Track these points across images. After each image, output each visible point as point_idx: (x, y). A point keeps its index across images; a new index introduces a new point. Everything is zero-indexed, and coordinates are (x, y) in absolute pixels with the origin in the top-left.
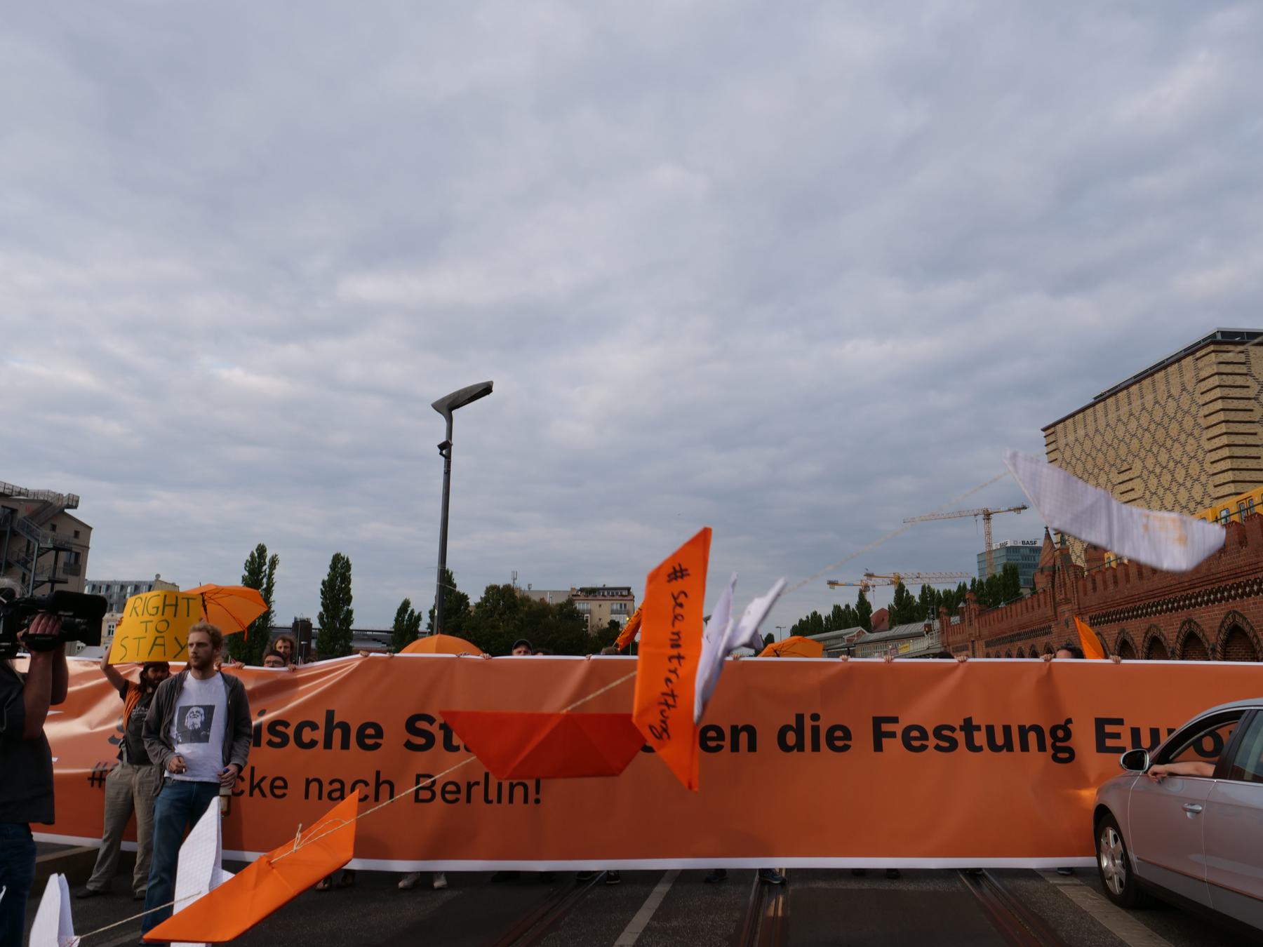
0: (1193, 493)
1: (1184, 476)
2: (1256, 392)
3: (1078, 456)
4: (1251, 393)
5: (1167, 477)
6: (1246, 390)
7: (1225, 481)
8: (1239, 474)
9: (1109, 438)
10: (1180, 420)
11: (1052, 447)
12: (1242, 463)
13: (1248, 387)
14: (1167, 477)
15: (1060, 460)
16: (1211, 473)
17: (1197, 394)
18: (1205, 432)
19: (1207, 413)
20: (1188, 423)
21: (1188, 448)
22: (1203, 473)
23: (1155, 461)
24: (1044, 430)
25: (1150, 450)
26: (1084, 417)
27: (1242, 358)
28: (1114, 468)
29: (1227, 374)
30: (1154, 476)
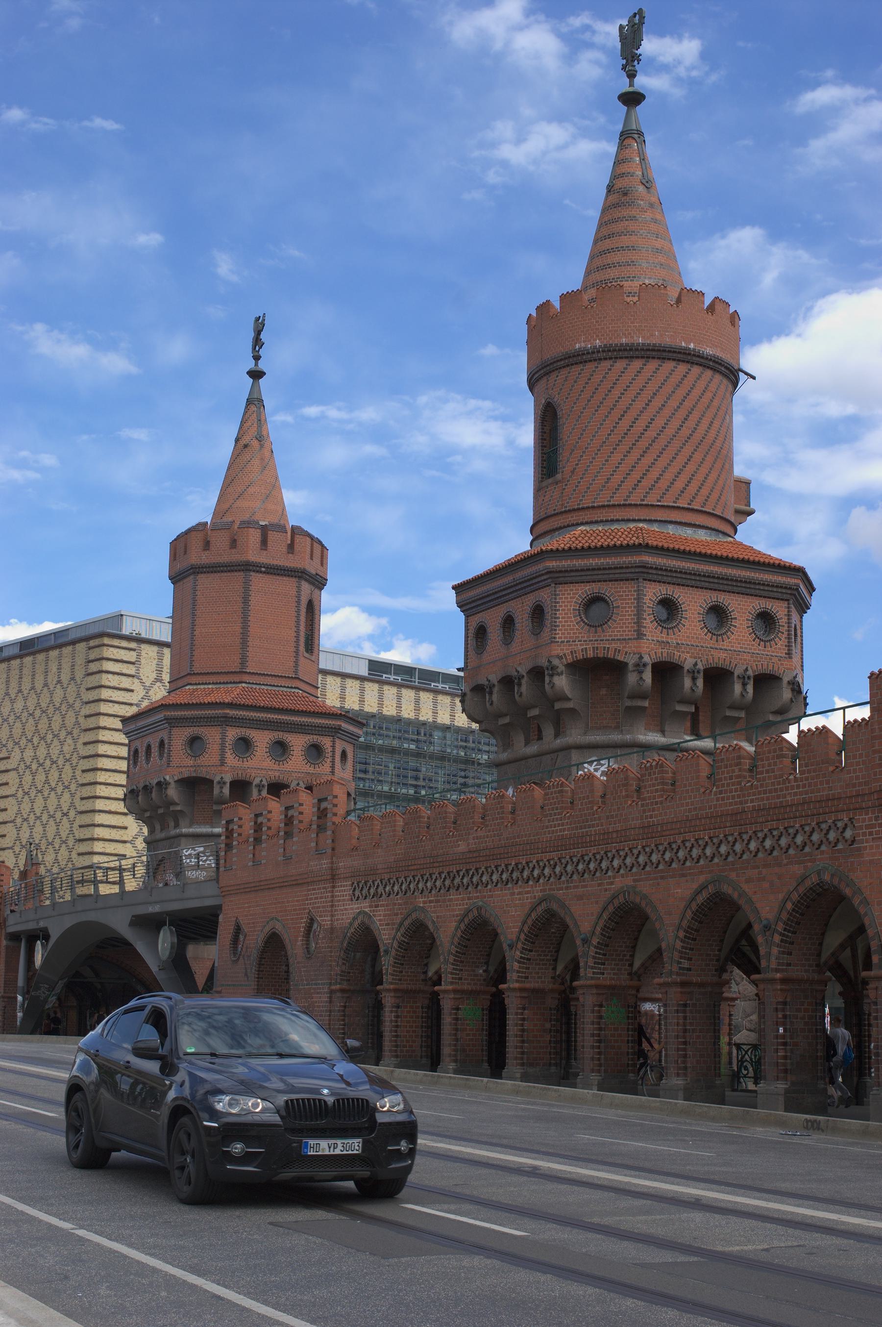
0: (62, 801)
2: (140, 698)
4: (134, 698)
5: (41, 777)
6: (130, 694)
8: (105, 789)
13: (132, 691)
14: (41, 777)
17: (83, 689)
18: (82, 734)
19: (88, 713)
21: (66, 748)
22: (74, 781)
23: (33, 754)
27: (131, 656)
29: (114, 673)
30: (29, 773)
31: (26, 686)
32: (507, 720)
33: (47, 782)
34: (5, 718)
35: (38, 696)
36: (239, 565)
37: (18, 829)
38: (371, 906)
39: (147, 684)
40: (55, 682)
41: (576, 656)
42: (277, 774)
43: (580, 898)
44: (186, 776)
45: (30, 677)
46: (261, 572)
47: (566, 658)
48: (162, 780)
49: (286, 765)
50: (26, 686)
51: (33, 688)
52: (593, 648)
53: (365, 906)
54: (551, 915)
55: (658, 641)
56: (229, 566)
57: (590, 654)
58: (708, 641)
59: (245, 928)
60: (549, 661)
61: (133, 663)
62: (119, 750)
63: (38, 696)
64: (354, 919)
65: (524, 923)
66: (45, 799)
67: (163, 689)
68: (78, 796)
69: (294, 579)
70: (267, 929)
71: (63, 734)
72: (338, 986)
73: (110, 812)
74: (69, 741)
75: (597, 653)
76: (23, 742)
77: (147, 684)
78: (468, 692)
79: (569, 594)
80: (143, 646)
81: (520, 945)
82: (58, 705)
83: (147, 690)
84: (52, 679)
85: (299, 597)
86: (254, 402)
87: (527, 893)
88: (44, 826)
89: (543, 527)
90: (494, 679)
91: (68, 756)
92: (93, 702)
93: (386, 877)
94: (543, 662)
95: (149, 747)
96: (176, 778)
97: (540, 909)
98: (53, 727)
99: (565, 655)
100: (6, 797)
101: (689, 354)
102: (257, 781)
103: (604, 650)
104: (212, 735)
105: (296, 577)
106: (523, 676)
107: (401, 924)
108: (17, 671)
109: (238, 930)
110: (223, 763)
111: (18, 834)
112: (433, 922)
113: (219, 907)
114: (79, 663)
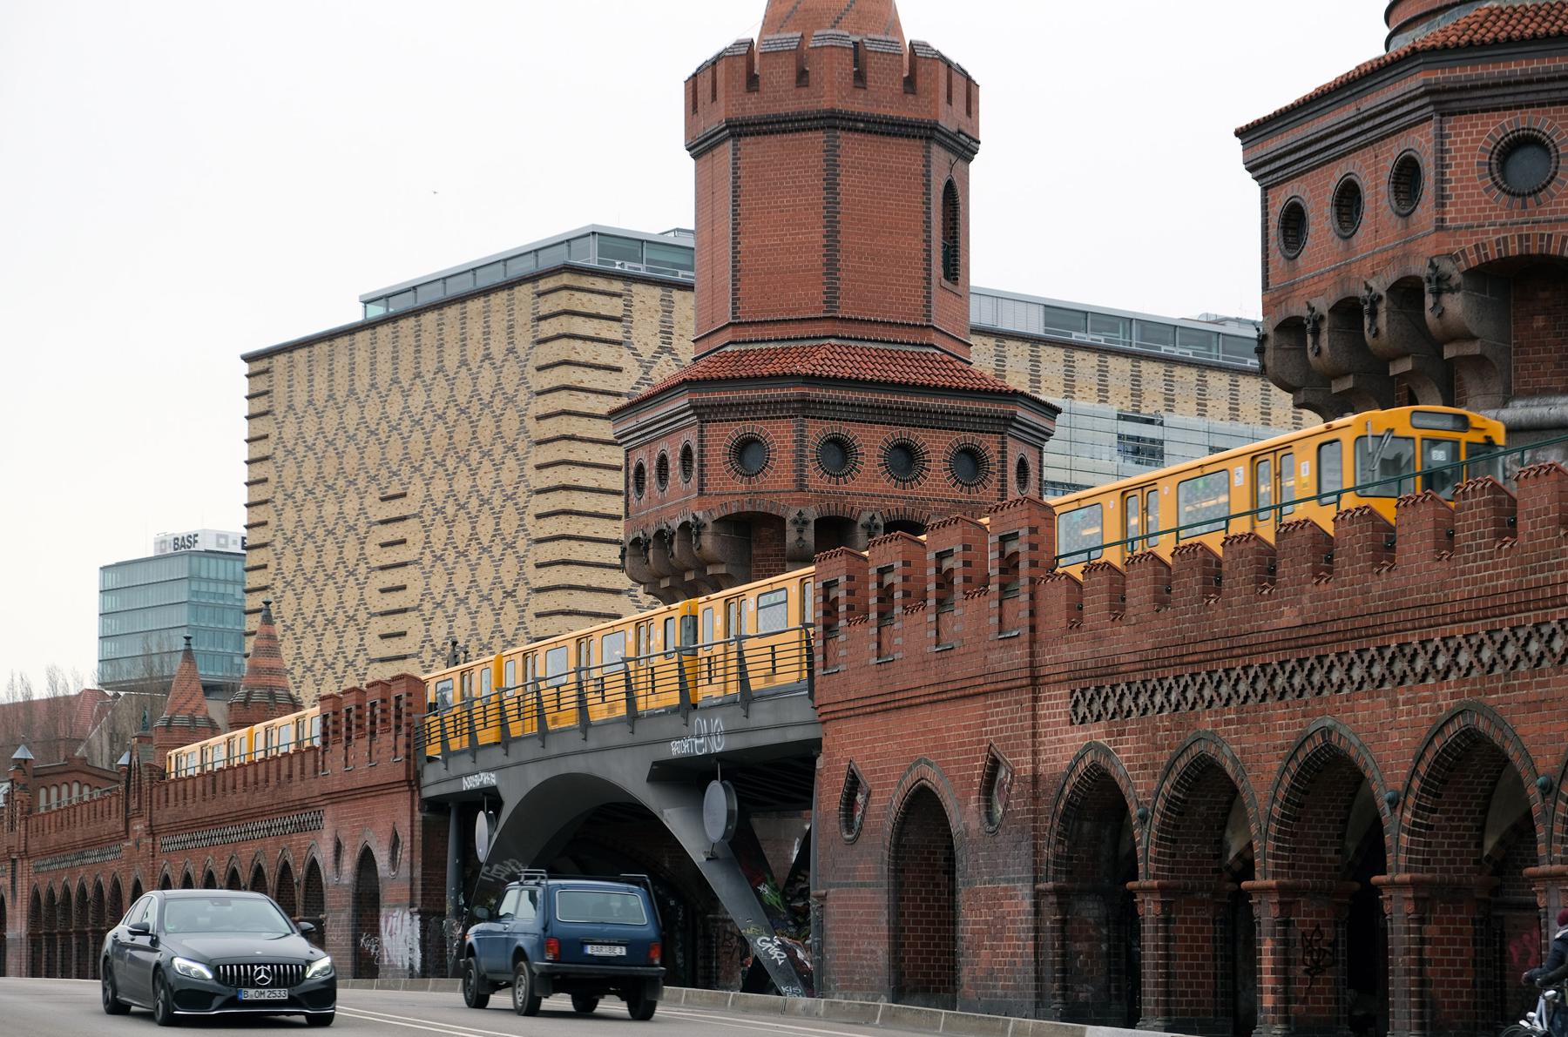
1: (492, 532)
3: (310, 441)
5: (463, 528)
7: (554, 559)
8: (579, 549)
9: (372, 414)
10: (498, 412)
11: (261, 404)
12: (586, 525)
13: (619, 370)
14: (463, 528)
15: (273, 438)
16: (534, 537)
17: (530, 369)
19: (541, 412)
20: (510, 425)
21: (506, 477)
22: (522, 534)
23: (447, 488)
24: (248, 359)
25: (442, 464)
26: (331, 356)
27: (614, 307)
28: (373, 487)
30: (442, 522)
31: (429, 365)
32: (1348, 383)
33: (474, 537)
34: (394, 423)
35: (451, 382)
36: (816, 118)
37: (428, 622)
38: (1109, 734)
39: (646, 357)
40: (479, 358)
41: (1486, 255)
42: (901, 504)
43: (1534, 706)
44: (734, 510)
45: (435, 349)
46: (857, 130)
47: (1466, 260)
48: (691, 520)
49: (917, 488)
50: (429, 365)
51: (440, 370)
52: (1520, 237)
53: (1097, 732)
54: (1471, 737)
56: (797, 121)
57: (1514, 249)
59: (867, 780)
60: (1432, 265)
61: (619, 320)
62: (599, 477)
63: (451, 382)
64: (1079, 758)
65: (1420, 758)
66: (473, 568)
67: (674, 367)
68: (530, 562)
69: (918, 142)
70: (909, 781)
71: (499, 450)
72: (1050, 885)
73: (589, 589)
74: (511, 462)
75: (1528, 247)
76: (428, 467)
77: (646, 357)
78: (1271, 333)
79: (1468, 134)
80: (636, 288)
81: (1411, 800)
82: (487, 399)
83: (647, 367)
84: (474, 352)
85: (927, 175)
87: (1425, 700)
88: (473, 615)
90: (1323, 305)
91: (510, 490)
92: (550, 391)
93: (1139, 677)
94: (1419, 268)
95: (663, 462)
96: (716, 516)
97: (1452, 729)
98: (481, 438)
99: (1463, 252)
100: (404, 564)
102: (865, 518)
103: (1542, 239)
104: (780, 435)
105: (921, 138)
106: (1380, 298)
107: (1170, 768)
108: (412, 340)
109: (854, 783)
110: (801, 487)
111: (427, 630)
112: (1234, 760)
113: (816, 744)
114: (521, 322)
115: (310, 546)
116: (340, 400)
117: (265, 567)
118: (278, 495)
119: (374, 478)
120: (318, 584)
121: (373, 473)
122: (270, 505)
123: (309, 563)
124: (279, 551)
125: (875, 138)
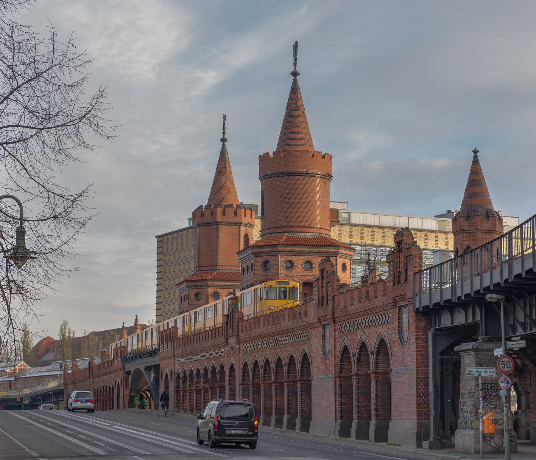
3: (172, 261)
15: (163, 260)
24: (157, 237)
34: (192, 257)
55: (285, 275)
58: (305, 273)
85: (239, 233)
86: (223, 152)
89: (265, 232)
101: (303, 173)
113: (159, 364)
115: (172, 291)
116: (179, 250)
117: (161, 296)
118: (164, 276)
119: (187, 272)
120: (174, 302)
121: (187, 270)
122: (162, 279)
123: (172, 296)
124: (164, 292)
125: (227, 226)
